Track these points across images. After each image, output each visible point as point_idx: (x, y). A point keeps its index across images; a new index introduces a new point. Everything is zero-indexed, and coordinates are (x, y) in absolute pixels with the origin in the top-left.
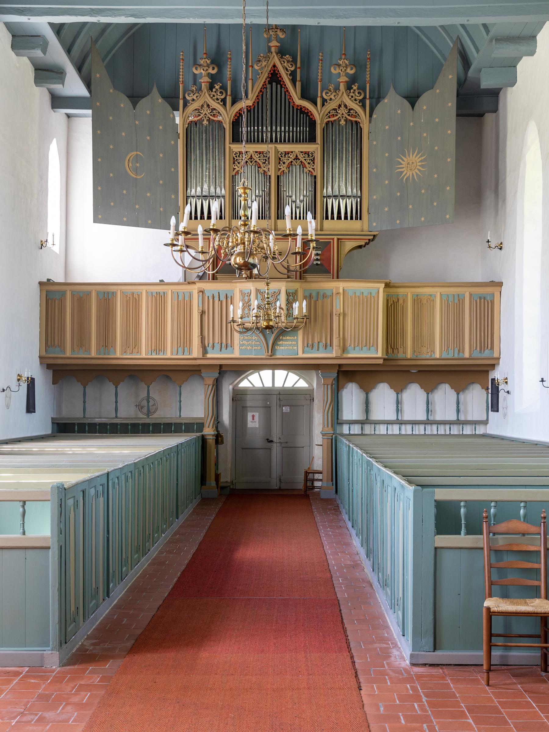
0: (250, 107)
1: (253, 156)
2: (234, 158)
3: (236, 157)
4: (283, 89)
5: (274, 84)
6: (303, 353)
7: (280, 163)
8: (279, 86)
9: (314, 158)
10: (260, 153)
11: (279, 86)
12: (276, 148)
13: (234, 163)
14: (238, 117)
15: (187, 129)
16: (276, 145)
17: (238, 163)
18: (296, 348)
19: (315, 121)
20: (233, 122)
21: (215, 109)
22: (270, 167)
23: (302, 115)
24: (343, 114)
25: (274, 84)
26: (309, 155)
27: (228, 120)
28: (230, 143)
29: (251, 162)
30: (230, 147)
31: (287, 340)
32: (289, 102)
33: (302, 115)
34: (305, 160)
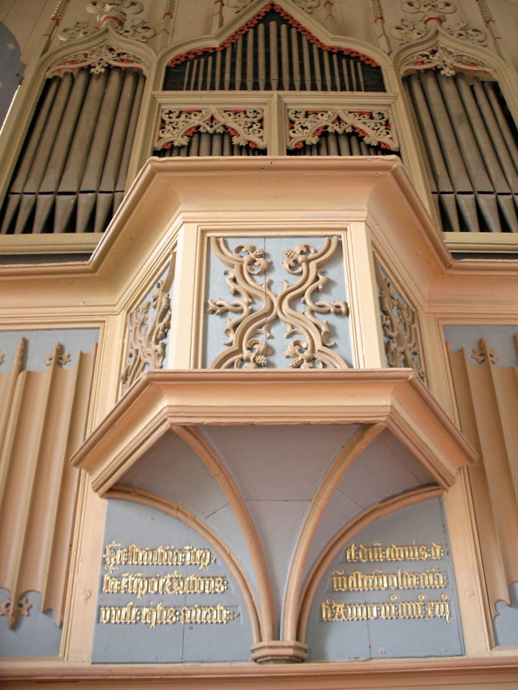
0: (214, 49)
1: (218, 117)
2: (163, 122)
3: (170, 118)
4: (294, 31)
5: (273, 25)
6: (494, 642)
7: (292, 128)
8: (284, 27)
9: (387, 122)
10: (236, 113)
11: (284, 27)
12: (279, 97)
13: (163, 128)
14: (184, 64)
15: (48, 83)
16: (281, 93)
17: (174, 128)
18: (441, 609)
19: (379, 68)
20: (168, 68)
21: (124, 54)
22: (264, 133)
23: (344, 61)
24: (444, 61)
25: (273, 25)
26: (372, 118)
27: (155, 59)
28: (155, 89)
29: (211, 127)
30: (153, 98)
31: (386, 567)
32: (310, 45)
33: (344, 61)
34: (364, 123)
